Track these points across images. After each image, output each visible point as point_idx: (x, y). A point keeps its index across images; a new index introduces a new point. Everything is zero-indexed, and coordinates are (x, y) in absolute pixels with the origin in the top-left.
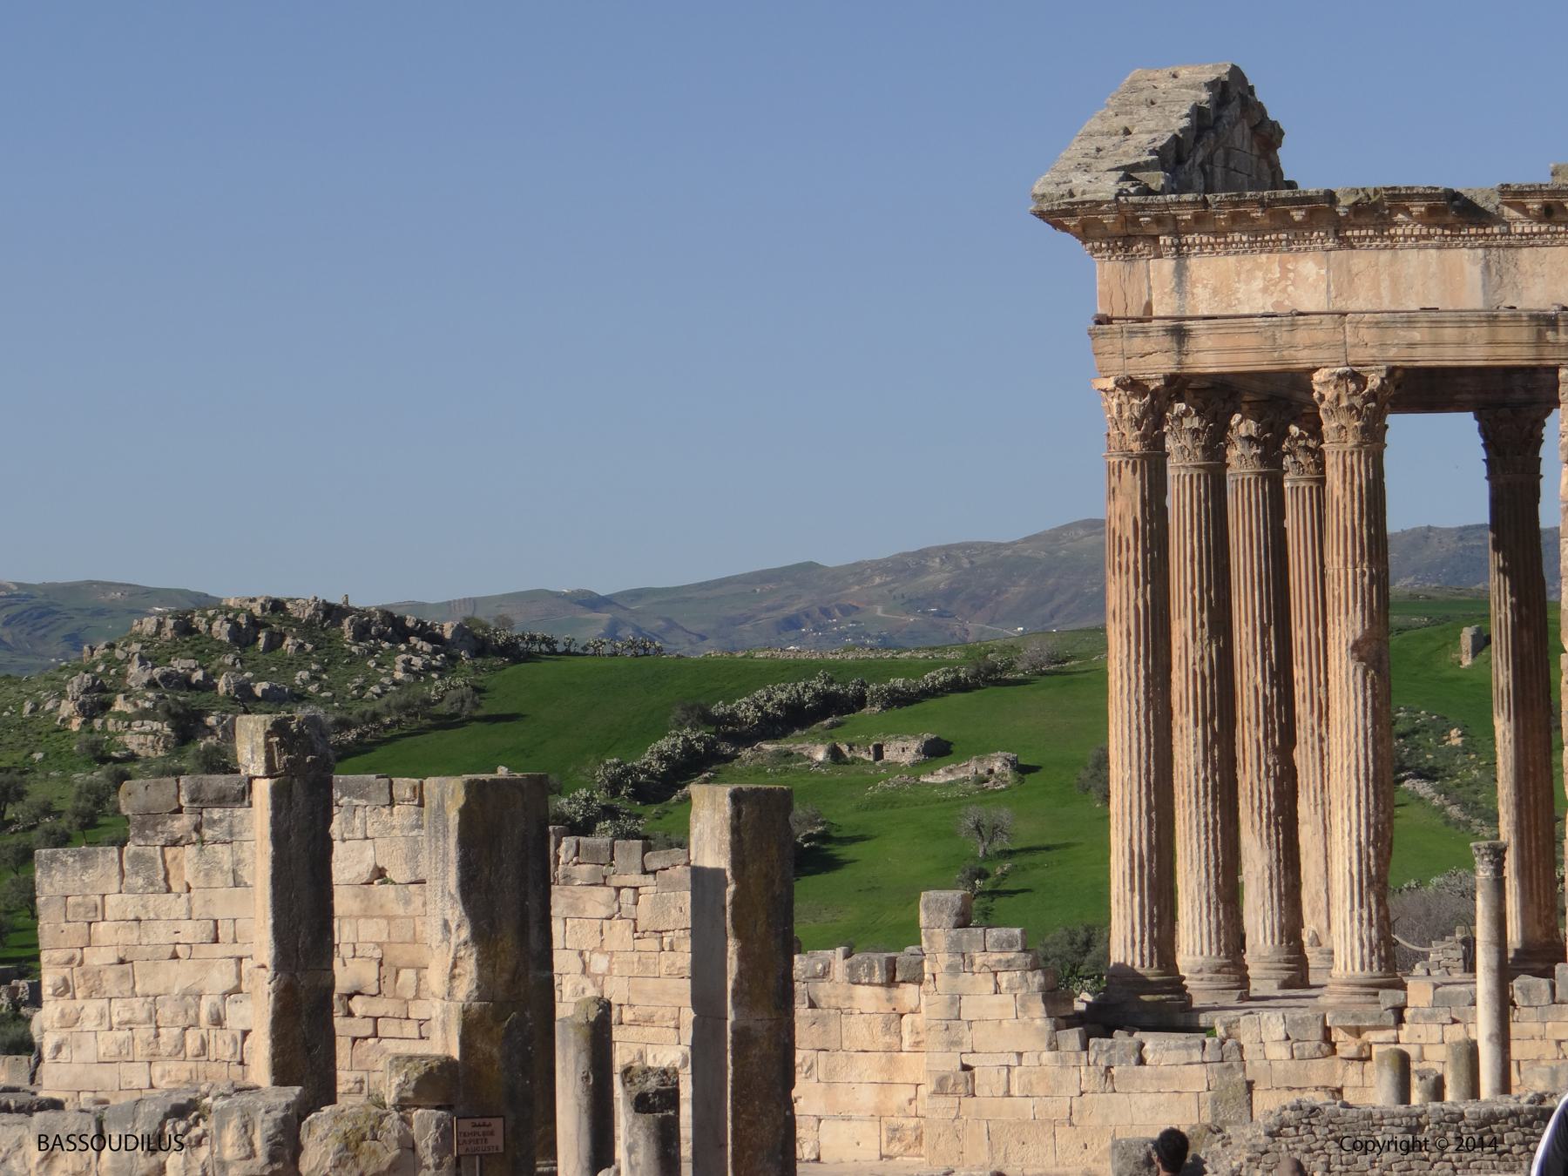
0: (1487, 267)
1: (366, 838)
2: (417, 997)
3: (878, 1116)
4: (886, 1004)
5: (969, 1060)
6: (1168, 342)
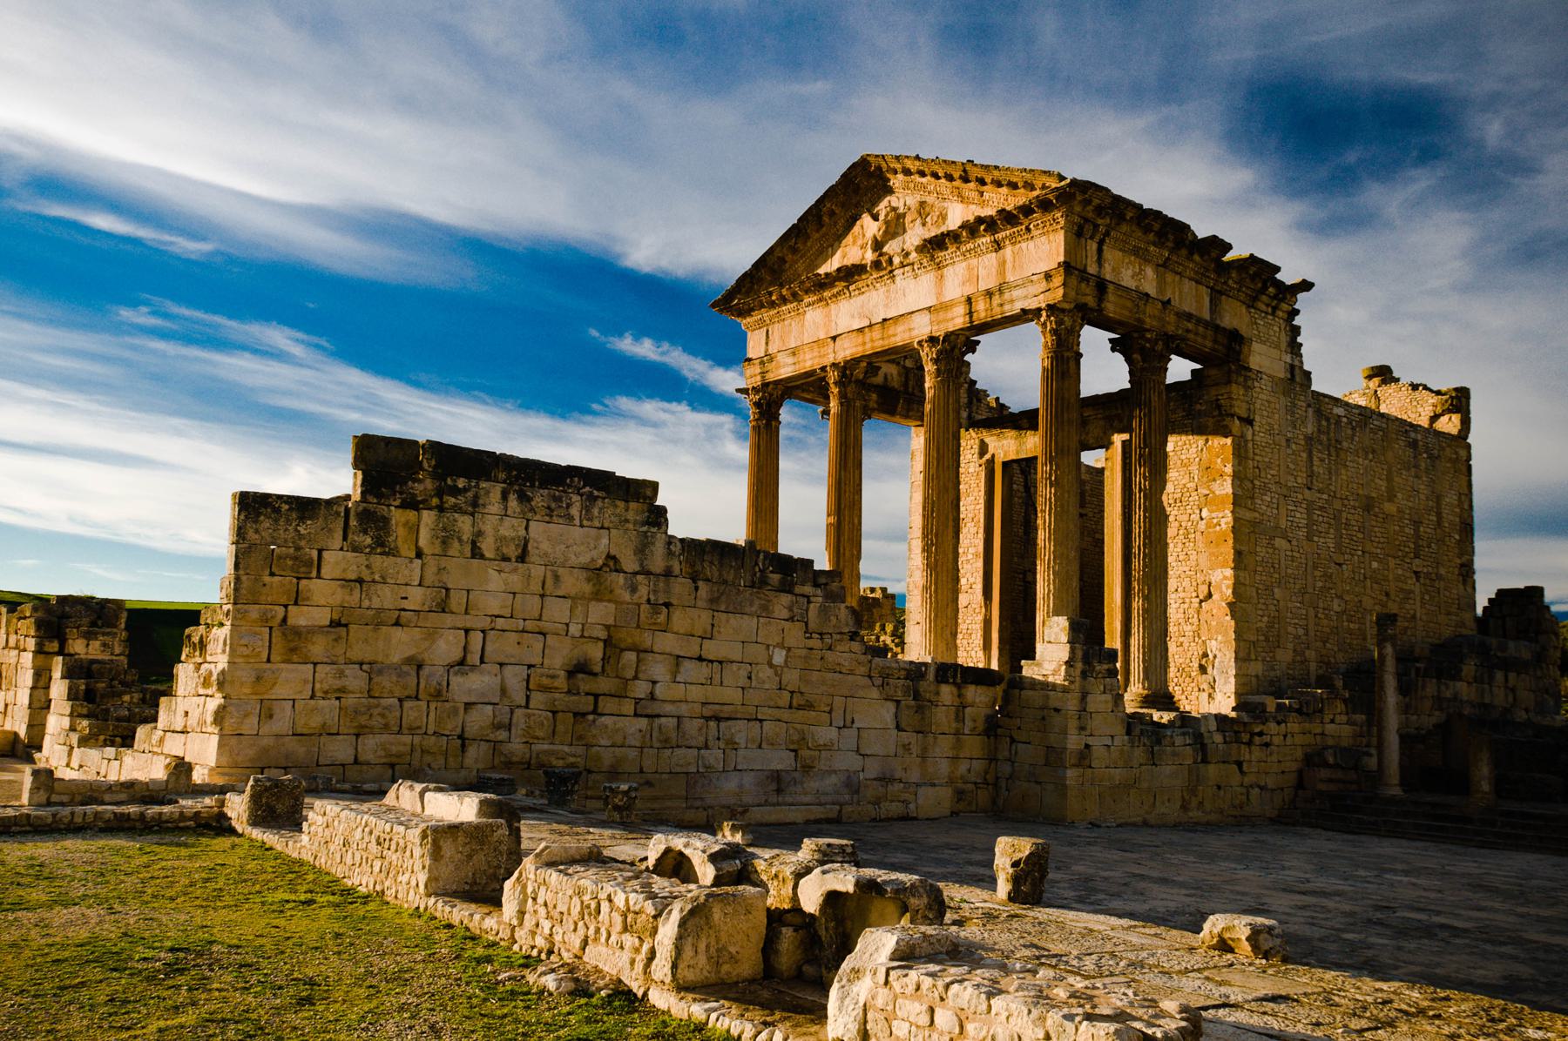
1: (602, 528)
2: (636, 678)
3: (951, 781)
5: (1090, 741)
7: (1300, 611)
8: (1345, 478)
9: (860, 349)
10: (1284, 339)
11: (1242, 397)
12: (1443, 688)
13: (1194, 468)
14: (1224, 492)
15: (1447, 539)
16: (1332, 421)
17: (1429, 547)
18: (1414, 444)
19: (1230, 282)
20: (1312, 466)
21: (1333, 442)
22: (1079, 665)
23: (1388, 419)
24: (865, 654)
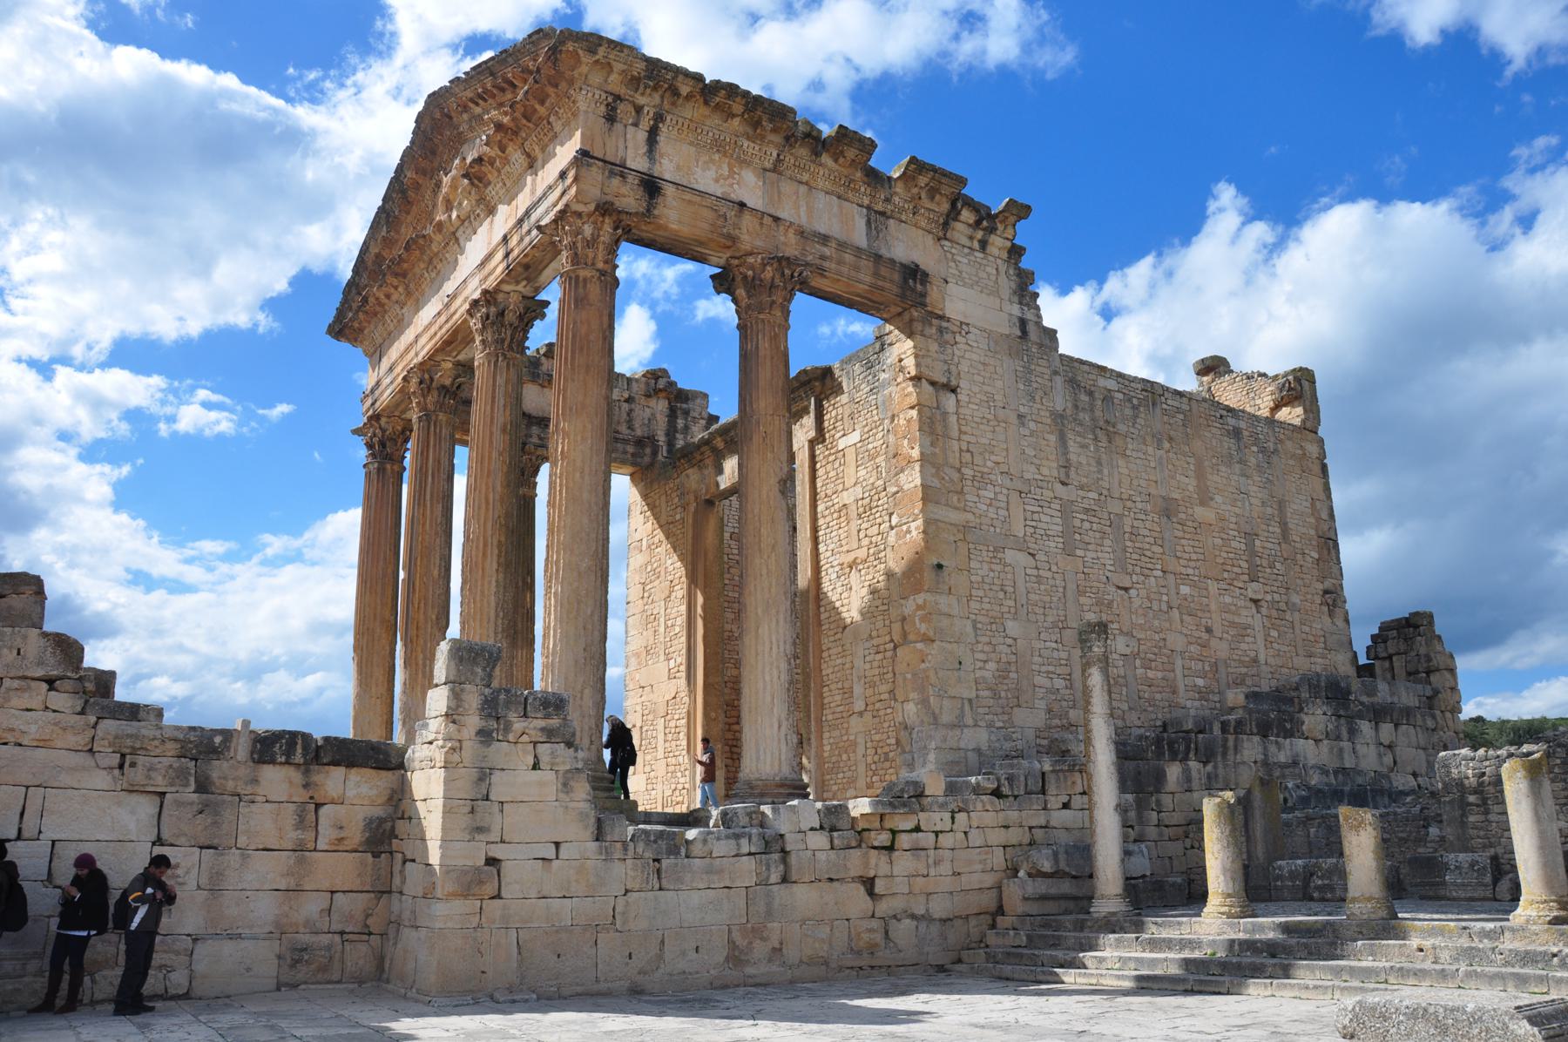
0: (869, 222)
3: (280, 930)
4: (301, 790)
5: (498, 852)
6: (640, 192)
7: (1055, 654)
8: (1125, 471)
9: (433, 342)
10: (1007, 285)
11: (935, 355)
12: (1273, 749)
13: (880, 460)
14: (912, 485)
15: (1299, 557)
16: (1097, 395)
17: (1272, 566)
18: (1236, 433)
19: (896, 199)
20: (1066, 453)
21: (1101, 423)
22: (473, 722)
23: (1190, 399)
24: (82, 713)
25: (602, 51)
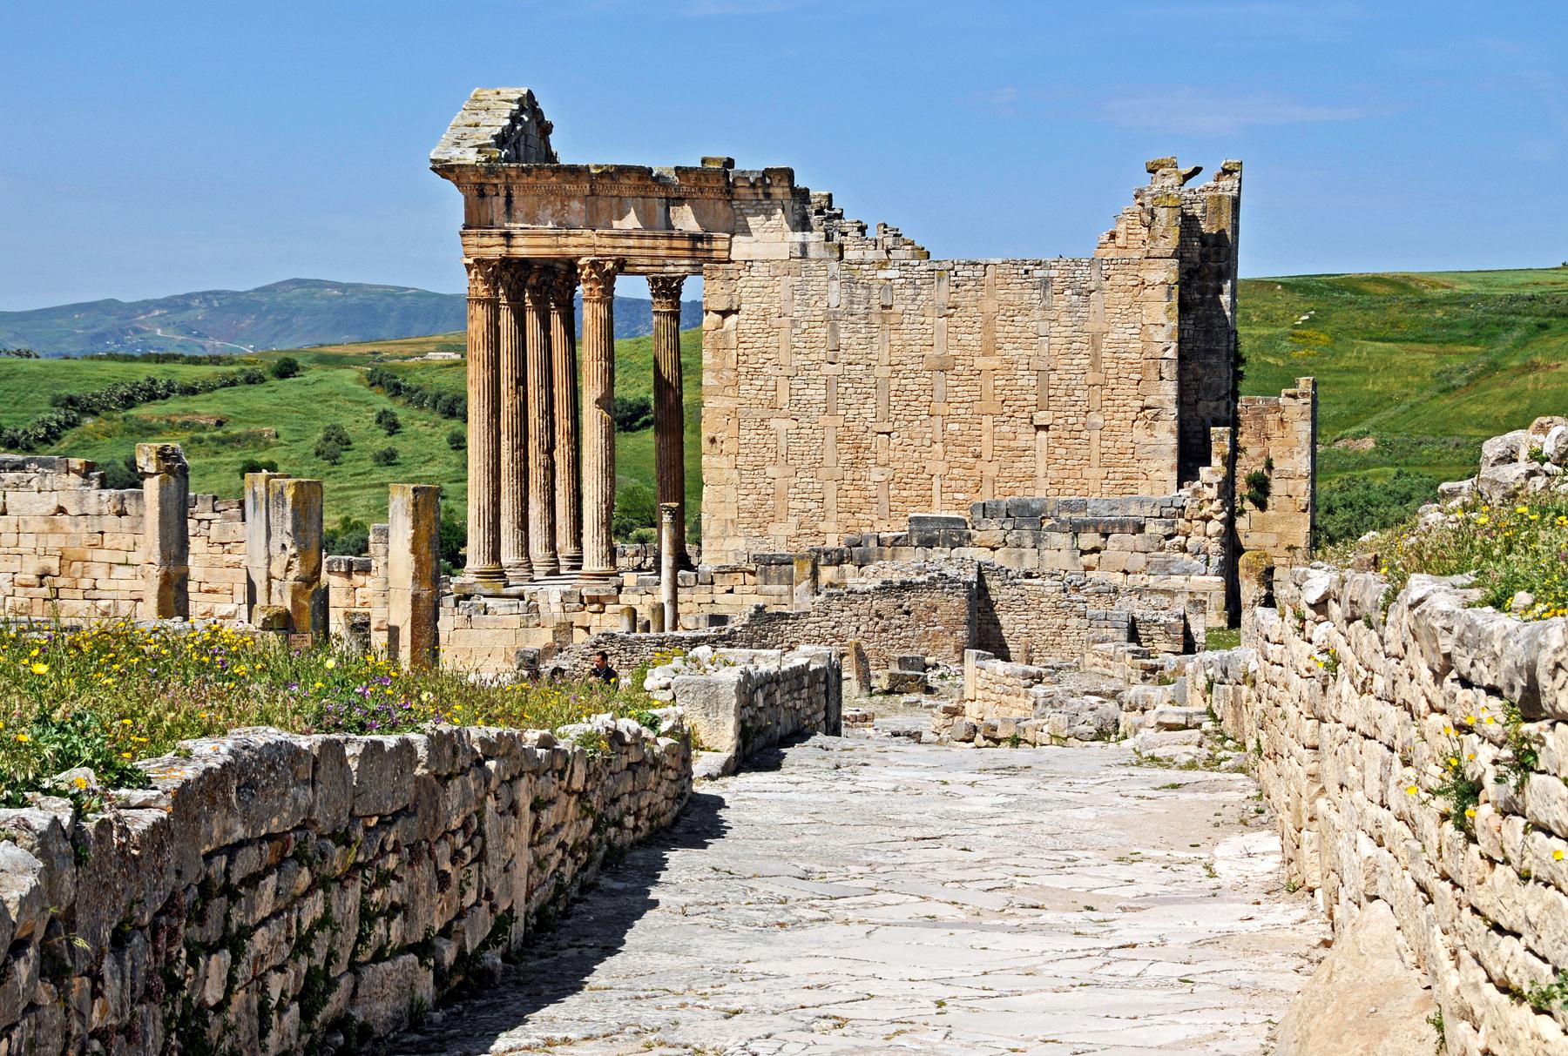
2: (82, 577)
6: (502, 240)
7: (811, 486)
16: (876, 286)
25: (457, 170)
